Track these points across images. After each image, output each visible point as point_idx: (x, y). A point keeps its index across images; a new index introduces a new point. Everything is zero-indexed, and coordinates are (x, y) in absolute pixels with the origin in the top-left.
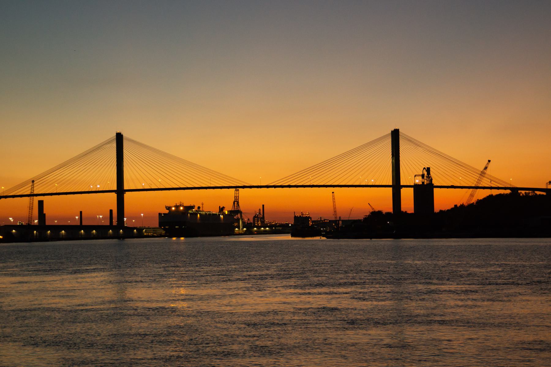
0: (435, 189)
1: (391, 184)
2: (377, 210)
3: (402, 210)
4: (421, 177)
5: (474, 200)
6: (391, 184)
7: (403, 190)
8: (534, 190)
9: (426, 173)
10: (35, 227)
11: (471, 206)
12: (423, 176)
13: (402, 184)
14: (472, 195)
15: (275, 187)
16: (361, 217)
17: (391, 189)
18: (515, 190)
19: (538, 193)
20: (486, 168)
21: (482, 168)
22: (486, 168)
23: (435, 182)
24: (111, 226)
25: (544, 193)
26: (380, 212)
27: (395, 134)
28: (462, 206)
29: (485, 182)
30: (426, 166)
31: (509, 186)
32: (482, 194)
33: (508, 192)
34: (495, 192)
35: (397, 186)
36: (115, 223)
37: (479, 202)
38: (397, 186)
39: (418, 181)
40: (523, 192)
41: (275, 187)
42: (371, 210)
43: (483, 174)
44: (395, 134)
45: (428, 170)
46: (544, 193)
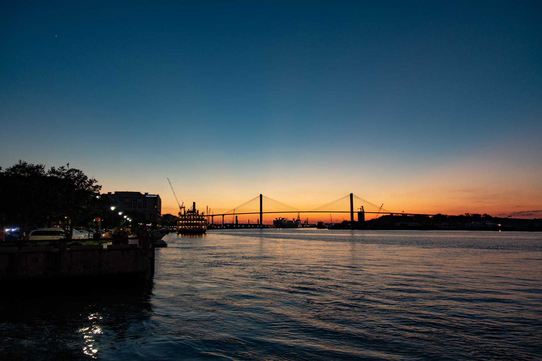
0: (365, 213)
1: (350, 211)
2: (345, 220)
3: (354, 220)
4: (360, 209)
5: (378, 217)
6: (350, 211)
7: (354, 213)
8: (398, 214)
9: (362, 208)
10: (235, 224)
11: (377, 219)
12: (361, 209)
13: (354, 211)
14: (377, 215)
15: (311, 212)
16: (340, 223)
17: (350, 213)
18: (392, 214)
19: (399, 215)
20: (382, 206)
21: (380, 207)
22: (382, 206)
23: (365, 211)
24: (258, 224)
25: (401, 215)
26: (346, 221)
27: (351, 195)
28: (374, 219)
29: (381, 211)
30: (362, 206)
31: (390, 212)
32: (381, 215)
33: (389, 214)
34: (385, 215)
35: (352, 212)
36: (259, 223)
37: (380, 218)
38: (352, 212)
39: (359, 210)
40: (394, 214)
41: (311, 212)
42: (344, 220)
43: (381, 208)
44: (351, 195)
45: (363, 207)
46: (401, 215)
